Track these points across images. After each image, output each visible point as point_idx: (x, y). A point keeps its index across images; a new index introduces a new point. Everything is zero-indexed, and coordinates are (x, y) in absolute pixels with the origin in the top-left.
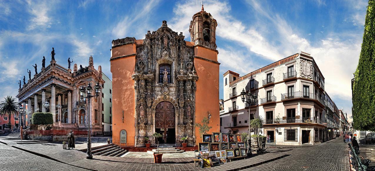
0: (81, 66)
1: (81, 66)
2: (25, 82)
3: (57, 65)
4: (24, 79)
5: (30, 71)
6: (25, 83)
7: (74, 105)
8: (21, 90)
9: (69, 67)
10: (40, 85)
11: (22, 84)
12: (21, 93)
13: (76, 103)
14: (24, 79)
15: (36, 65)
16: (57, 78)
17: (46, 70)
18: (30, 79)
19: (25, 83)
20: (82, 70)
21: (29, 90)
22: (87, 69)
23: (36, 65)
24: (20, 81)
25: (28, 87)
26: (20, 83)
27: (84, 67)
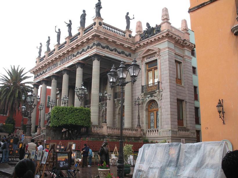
0: (148, 24)
1: (148, 24)
2: (50, 46)
3: (104, 25)
4: (48, 42)
5: (59, 30)
6: (48, 49)
7: (139, 93)
8: (41, 59)
9: (128, 27)
10: (74, 56)
11: (44, 49)
12: (40, 67)
13: (141, 88)
14: (48, 42)
15: (70, 21)
16: (104, 45)
17: (86, 31)
18: (59, 43)
19: (48, 49)
20: (151, 31)
21: (55, 62)
22: (158, 29)
23: (70, 21)
24: (41, 44)
25: (55, 56)
26: (41, 47)
27: (153, 25)
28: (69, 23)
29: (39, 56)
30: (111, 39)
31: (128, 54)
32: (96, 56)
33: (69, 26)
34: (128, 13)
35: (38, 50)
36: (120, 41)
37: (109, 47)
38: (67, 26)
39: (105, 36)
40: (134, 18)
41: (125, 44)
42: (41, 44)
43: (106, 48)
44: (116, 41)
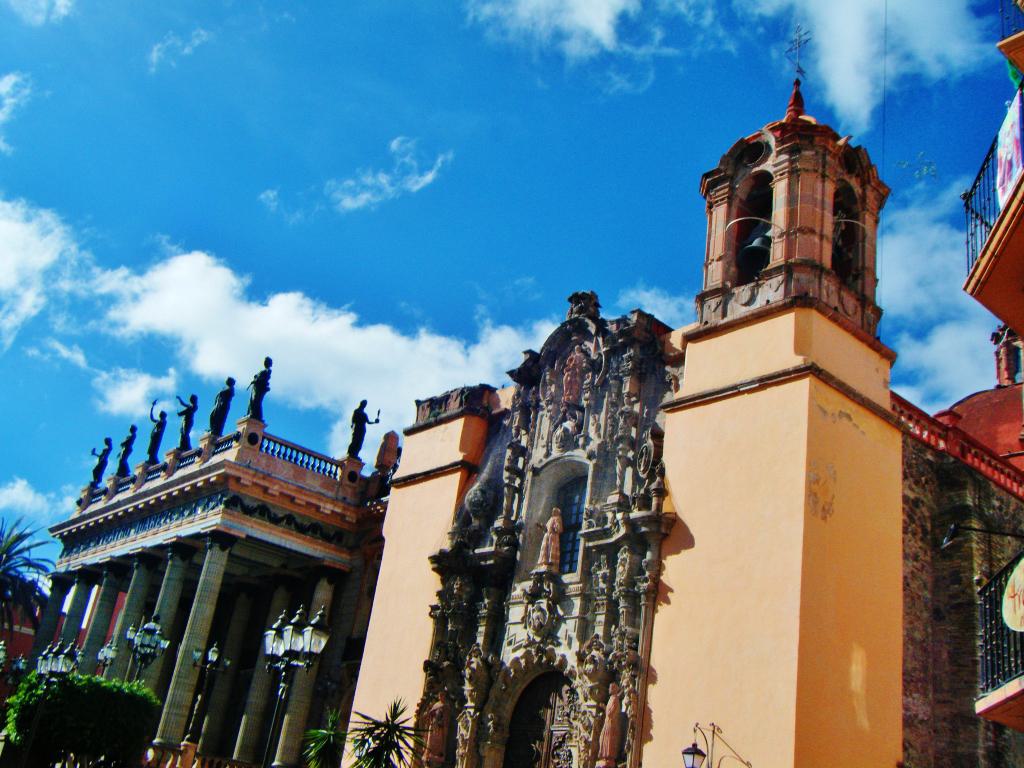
4: (128, 445)
6: (124, 469)
14: (128, 445)
15: (194, 399)
19: (124, 469)
23: (194, 399)
24: (108, 442)
26: (106, 453)
28: (191, 405)
29: (94, 485)
30: (276, 487)
31: (332, 533)
32: (219, 538)
33: (189, 414)
34: (364, 404)
35: (97, 461)
36: (305, 495)
37: (268, 510)
38: (180, 414)
39: (255, 480)
40: (377, 421)
41: (322, 504)
42: (108, 442)
43: (257, 514)
44: (293, 494)
